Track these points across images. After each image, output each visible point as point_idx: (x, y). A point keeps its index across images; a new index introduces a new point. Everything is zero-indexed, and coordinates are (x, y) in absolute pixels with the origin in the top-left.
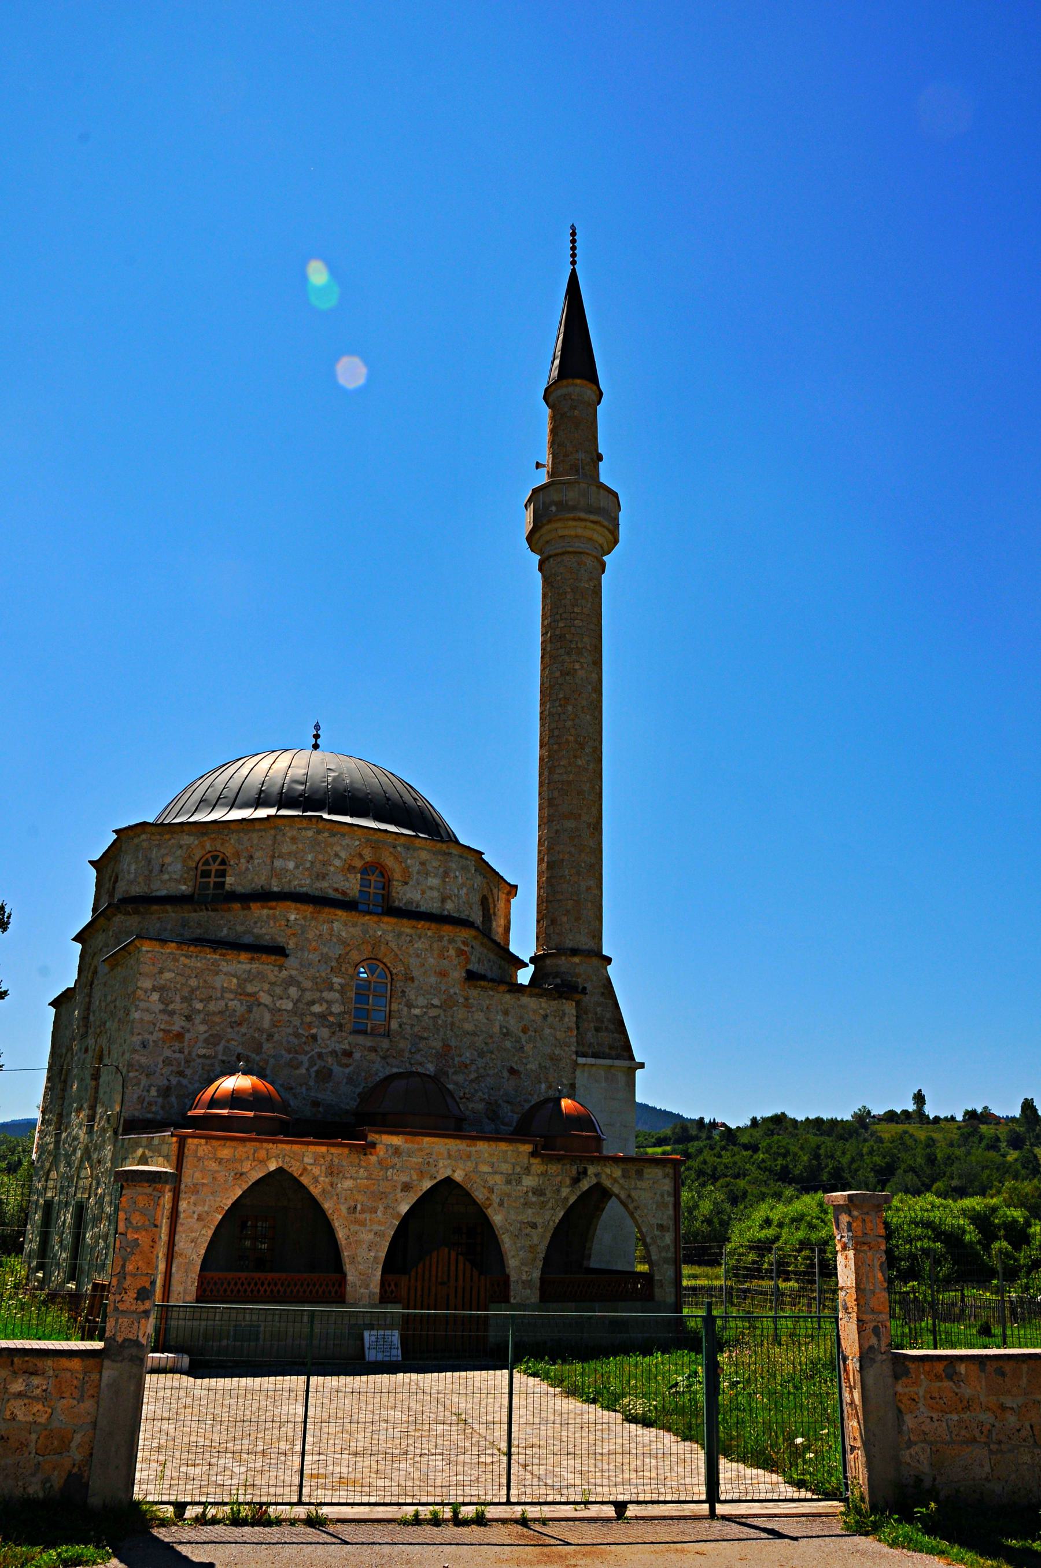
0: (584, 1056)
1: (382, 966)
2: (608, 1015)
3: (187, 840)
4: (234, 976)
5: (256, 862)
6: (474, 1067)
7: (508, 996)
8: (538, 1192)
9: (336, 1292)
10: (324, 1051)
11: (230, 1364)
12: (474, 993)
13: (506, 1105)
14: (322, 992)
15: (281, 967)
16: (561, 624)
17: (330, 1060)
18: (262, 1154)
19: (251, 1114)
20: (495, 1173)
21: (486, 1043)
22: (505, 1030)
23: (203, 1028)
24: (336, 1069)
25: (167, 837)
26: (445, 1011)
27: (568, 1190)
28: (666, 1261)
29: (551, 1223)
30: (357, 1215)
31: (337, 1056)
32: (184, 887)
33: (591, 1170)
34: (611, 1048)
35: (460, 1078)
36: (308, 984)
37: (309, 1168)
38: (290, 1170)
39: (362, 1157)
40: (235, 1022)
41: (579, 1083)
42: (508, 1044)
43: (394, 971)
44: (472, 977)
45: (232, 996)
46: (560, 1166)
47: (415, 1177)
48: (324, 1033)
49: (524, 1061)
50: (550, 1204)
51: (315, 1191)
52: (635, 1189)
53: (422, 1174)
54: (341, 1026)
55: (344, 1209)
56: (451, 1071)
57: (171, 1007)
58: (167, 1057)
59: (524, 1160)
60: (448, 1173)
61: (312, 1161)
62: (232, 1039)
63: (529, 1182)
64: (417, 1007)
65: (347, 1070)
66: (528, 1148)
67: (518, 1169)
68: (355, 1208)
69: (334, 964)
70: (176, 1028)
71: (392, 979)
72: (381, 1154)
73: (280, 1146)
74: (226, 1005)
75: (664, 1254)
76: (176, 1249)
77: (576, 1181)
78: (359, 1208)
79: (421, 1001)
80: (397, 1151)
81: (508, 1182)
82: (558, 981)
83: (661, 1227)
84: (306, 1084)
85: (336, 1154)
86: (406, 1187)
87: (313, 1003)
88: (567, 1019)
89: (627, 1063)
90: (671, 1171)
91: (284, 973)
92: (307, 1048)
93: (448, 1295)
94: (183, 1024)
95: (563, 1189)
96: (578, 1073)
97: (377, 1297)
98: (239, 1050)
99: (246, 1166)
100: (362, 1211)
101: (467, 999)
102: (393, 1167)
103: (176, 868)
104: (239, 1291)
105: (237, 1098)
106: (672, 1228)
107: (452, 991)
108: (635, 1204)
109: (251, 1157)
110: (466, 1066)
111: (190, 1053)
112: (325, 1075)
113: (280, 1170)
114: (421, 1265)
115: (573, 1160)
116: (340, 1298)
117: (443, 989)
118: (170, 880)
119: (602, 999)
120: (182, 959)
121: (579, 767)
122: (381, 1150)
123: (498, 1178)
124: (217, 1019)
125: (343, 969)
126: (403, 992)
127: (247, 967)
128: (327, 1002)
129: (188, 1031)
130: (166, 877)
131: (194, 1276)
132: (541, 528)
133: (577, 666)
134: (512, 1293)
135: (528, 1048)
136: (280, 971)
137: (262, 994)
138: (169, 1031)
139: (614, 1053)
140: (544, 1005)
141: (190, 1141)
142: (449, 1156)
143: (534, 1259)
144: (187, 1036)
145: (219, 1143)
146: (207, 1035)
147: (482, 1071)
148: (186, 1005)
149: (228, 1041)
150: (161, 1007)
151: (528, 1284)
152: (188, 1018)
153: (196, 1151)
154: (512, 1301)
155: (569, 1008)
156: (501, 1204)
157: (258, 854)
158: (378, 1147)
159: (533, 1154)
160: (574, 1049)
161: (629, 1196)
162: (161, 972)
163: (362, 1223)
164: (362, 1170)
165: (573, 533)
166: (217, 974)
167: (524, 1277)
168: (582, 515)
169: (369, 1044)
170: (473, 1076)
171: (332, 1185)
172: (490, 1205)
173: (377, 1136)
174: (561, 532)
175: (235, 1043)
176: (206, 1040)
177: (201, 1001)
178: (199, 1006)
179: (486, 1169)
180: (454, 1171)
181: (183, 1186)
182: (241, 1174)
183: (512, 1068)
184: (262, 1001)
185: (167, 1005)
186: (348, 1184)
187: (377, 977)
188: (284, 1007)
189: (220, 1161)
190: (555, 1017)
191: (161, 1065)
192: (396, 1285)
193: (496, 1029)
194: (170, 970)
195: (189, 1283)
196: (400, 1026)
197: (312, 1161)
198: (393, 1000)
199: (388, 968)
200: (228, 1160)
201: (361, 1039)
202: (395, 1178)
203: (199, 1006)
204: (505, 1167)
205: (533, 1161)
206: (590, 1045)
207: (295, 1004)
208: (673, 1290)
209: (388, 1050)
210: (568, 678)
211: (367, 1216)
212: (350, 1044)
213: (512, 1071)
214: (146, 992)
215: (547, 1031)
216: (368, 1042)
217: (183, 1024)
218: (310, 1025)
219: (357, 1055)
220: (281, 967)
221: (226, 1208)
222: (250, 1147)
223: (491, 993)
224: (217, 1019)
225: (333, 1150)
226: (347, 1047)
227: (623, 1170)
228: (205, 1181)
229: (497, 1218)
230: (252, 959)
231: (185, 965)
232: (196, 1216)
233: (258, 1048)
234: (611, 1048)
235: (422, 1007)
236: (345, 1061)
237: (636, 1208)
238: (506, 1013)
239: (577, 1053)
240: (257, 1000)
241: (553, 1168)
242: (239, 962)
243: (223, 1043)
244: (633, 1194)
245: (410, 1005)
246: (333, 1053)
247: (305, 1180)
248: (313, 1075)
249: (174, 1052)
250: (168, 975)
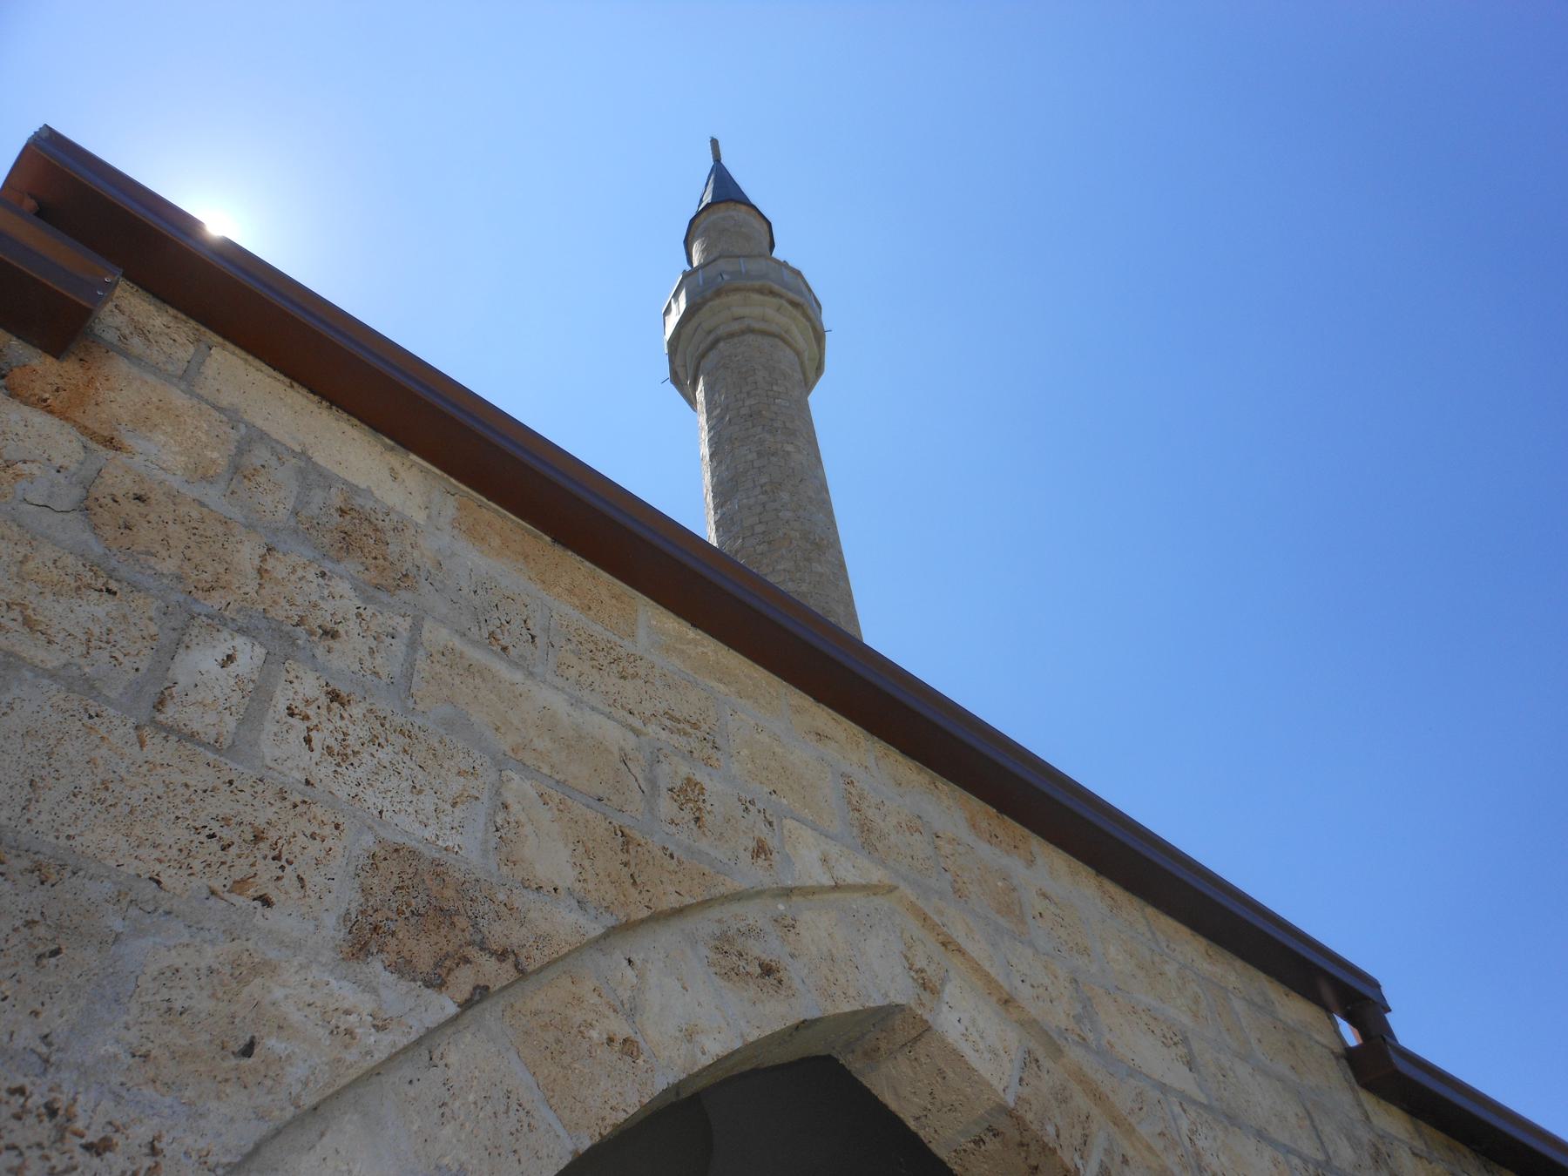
80: (354, 532)
121: (821, 575)
133: (789, 448)
168: (776, 287)
174: (738, 311)
202: (283, 751)
210: (773, 459)
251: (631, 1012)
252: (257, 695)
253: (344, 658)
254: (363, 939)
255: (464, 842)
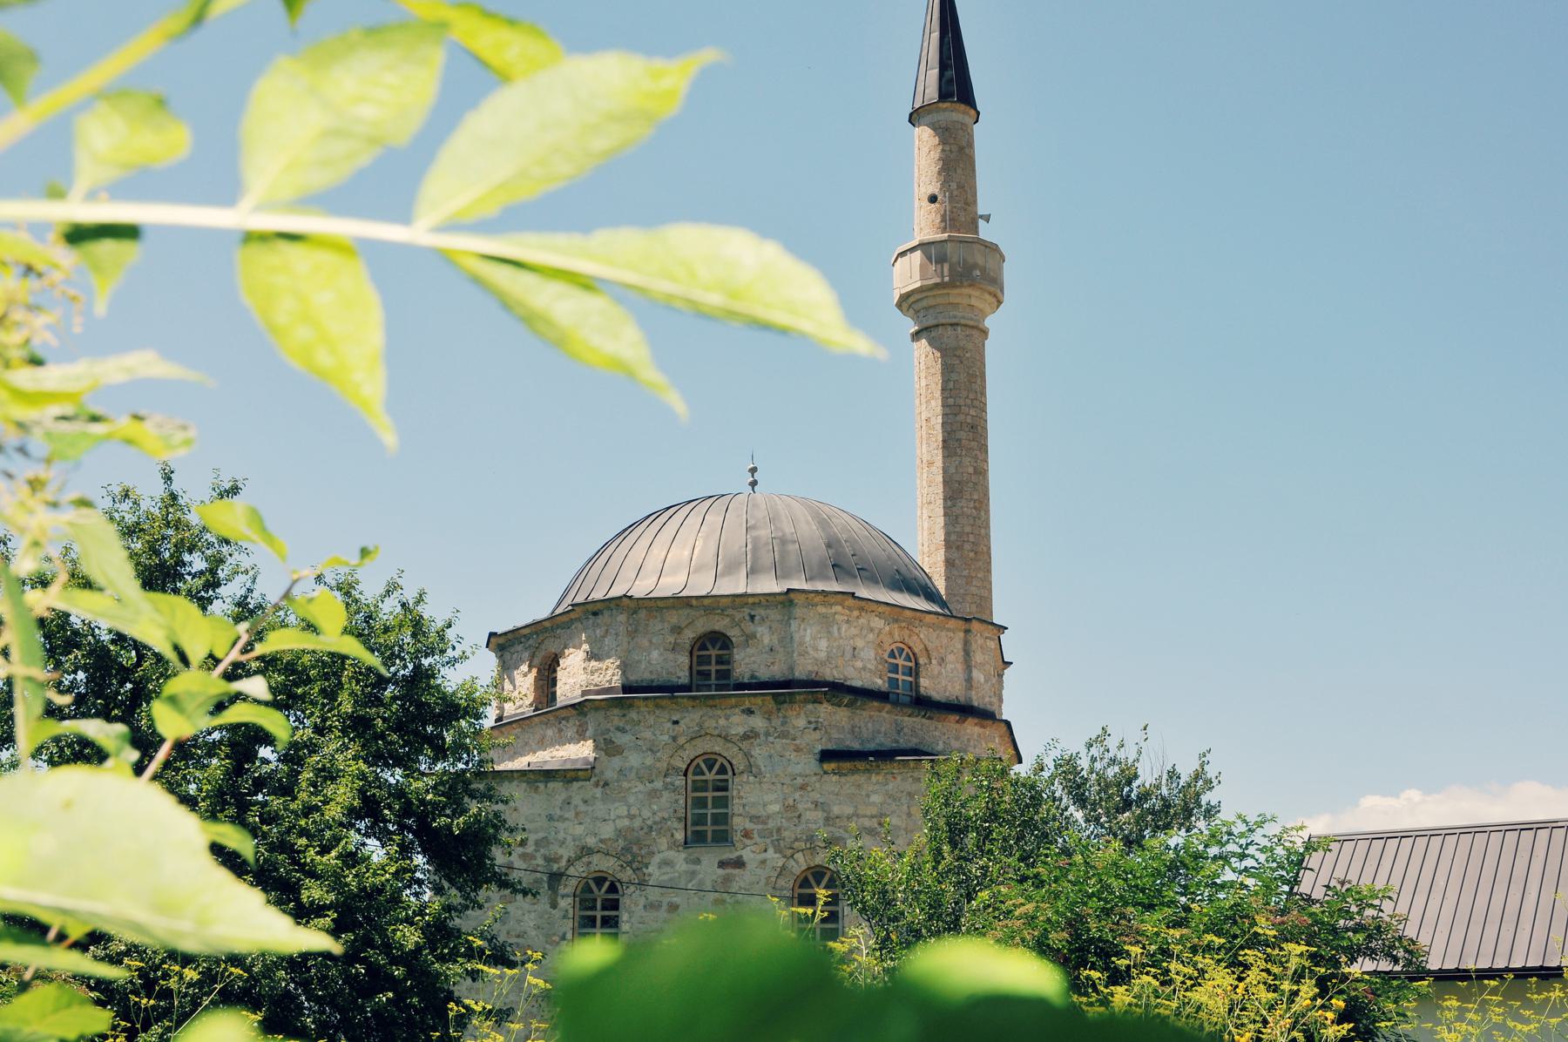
3: (878, 623)
5: (949, 666)
16: (972, 412)
25: (856, 613)
32: (880, 682)
103: (869, 655)
118: (864, 668)
130: (859, 664)
132: (955, 287)
157: (950, 658)
165: (965, 301)
174: (973, 302)
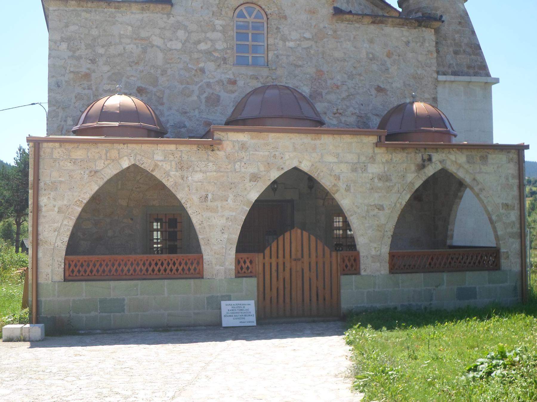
0: (444, 74)
1: (258, 8)
2: (466, 41)
4: (128, 25)
6: (345, 87)
7: (372, 27)
8: (384, 178)
9: (195, 269)
10: (211, 81)
11: (98, 331)
12: (342, 26)
13: (375, 117)
14: (206, 33)
15: (169, 14)
17: (217, 88)
18: (114, 153)
19: (116, 124)
20: (341, 162)
21: (355, 67)
22: (371, 56)
23: (106, 68)
24: (224, 95)
26: (316, 42)
27: (414, 175)
28: (512, 235)
29: (398, 205)
30: (209, 203)
31: (223, 84)
33: (436, 157)
34: (469, 67)
35: (332, 97)
36: (193, 27)
37: (160, 164)
38: (142, 166)
39: (210, 153)
40: (133, 62)
41: (440, 97)
42: (374, 67)
43: (269, 12)
44: (338, 11)
45: (128, 41)
46: (405, 155)
47: (262, 169)
48: (210, 66)
49: (390, 80)
50: (396, 189)
51: (169, 184)
52: (480, 172)
53: (269, 166)
54: (224, 59)
55: (195, 198)
56: (324, 92)
57: (78, 53)
58: (79, 94)
59: (369, 151)
60: (295, 164)
61: (161, 158)
62: (132, 76)
63: (374, 169)
64: (292, 40)
65: (233, 96)
66: (373, 139)
67: (363, 159)
68: (207, 197)
69: (215, 9)
70: (84, 70)
71: (268, 19)
72: (229, 149)
73: (131, 146)
74: (124, 48)
75: (509, 230)
76: (40, 237)
77: (422, 167)
78: (210, 197)
79: (295, 35)
80: (243, 147)
81: (354, 170)
82: (420, 14)
83: (506, 206)
84: (198, 108)
85: (186, 151)
86: (255, 178)
87: (199, 42)
88: (427, 45)
89: (483, 79)
90: (515, 156)
91: (172, 20)
92: (196, 79)
93: (303, 270)
94: (89, 66)
95: (408, 175)
96: (440, 89)
97: (233, 273)
98: (139, 84)
99: (100, 165)
100: (214, 200)
101: (335, 32)
102: (241, 160)
104: (104, 271)
105: (105, 112)
106: (517, 206)
107: (321, 26)
108: (480, 187)
109: (104, 157)
110: (338, 87)
111: (97, 89)
112: (214, 101)
113: (135, 169)
114: (274, 245)
115: (417, 149)
116: (199, 275)
117: (314, 24)
119: (459, 27)
120: (84, 14)
122: (228, 146)
123: (343, 167)
124: (117, 60)
125: (223, 13)
126: (278, 28)
127: (139, 16)
128: (211, 40)
129: (94, 71)
131: (60, 259)
134: (362, 267)
135: (393, 70)
136: (168, 18)
137: (154, 38)
138: (78, 73)
139: (471, 71)
140: (406, 33)
141: (45, 145)
142: (295, 149)
143: (383, 236)
144: (93, 75)
145: (73, 145)
146: (110, 74)
147: (352, 90)
148: (90, 51)
149: (128, 77)
150: (70, 54)
151: (376, 258)
152: (93, 61)
153: (52, 153)
154: (363, 273)
155: (429, 34)
156: (348, 189)
158: (225, 143)
159: (377, 145)
160: (434, 68)
161: (474, 179)
162: (67, 26)
163: (214, 210)
164: (210, 164)
166: (114, 24)
167: (373, 253)
169: (251, 73)
170: (344, 95)
171: (182, 179)
172: (337, 191)
173: (223, 134)
175: (135, 79)
176: (109, 78)
177: (103, 46)
178: (101, 51)
179: (330, 159)
180: (300, 162)
181: (42, 185)
182: (96, 172)
183: (378, 86)
184: (155, 43)
185: (74, 52)
186: (198, 176)
187: (254, 18)
188: (174, 47)
189: (75, 161)
190: (417, 43)
191: (74, 100)
192: (251, 262)
193: (363, 55)
194: (74, 24)
195: (56, 266)
196: (277, 57)
197: (161, 158)
198: (269, 35)
199: (264, 10)
200: (82, 160)
201: (243, 70)
202: (243, 170)
203: (101, 51)
204: (351, 157)
205: (377, 150)
206: (450, 66)
207: (183, 44)
208: (519, 260)
209: (268, 77)
211: (219, 204)
212: (234, 74)
213: (379, 89)
214: (55, 43)
215: (410, 55)
216: (250, 71)
217: (89, 66)
218: (198, 60)
219: (241, 83)
220: (169, 14)
221: (85, 201)
222: (102, 149)
223: (357, 25)
224: (117, 60)
225: (182, 148)
226: (232, 77)
227: (467, 157)
228: (60, 179)
229: (345, 202)
230: (143, 9)
231: (86, 19)
232: (56, 209)
233: (155, 82)
234: (469, 67)
235: (295, 40)
236: (230, 87)
237: (481, 190)
238: (371, 41)
239: (438, 73)
240: (150, 42)
241: (399, 157)
242: (132, 13)
243: (124, 79)
244: (479, 177)
245: (284, 39)
246: (220, 82)
247: (157, 174)
248: (204, 101)
249: (84, 89)
250: (72, 28)
251: (269, 177)
252: (240, 167)
253: (245, 160)
254: (250, 181)
255: (255, 170)
